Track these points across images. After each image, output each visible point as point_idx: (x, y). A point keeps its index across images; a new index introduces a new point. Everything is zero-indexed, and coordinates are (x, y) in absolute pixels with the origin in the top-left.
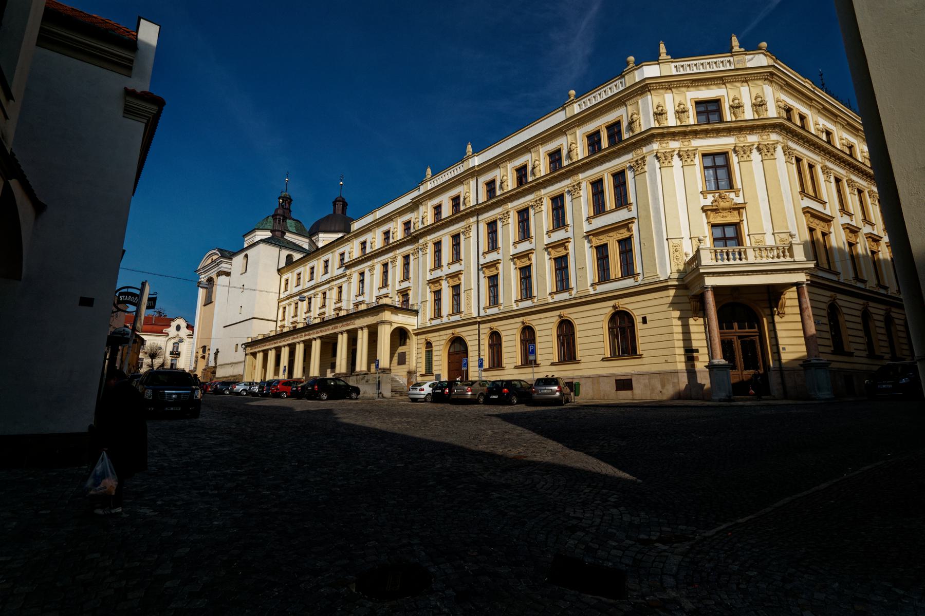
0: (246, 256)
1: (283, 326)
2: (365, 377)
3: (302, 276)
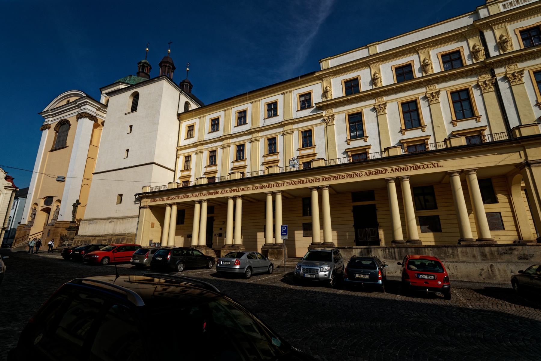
0: (136, 96)
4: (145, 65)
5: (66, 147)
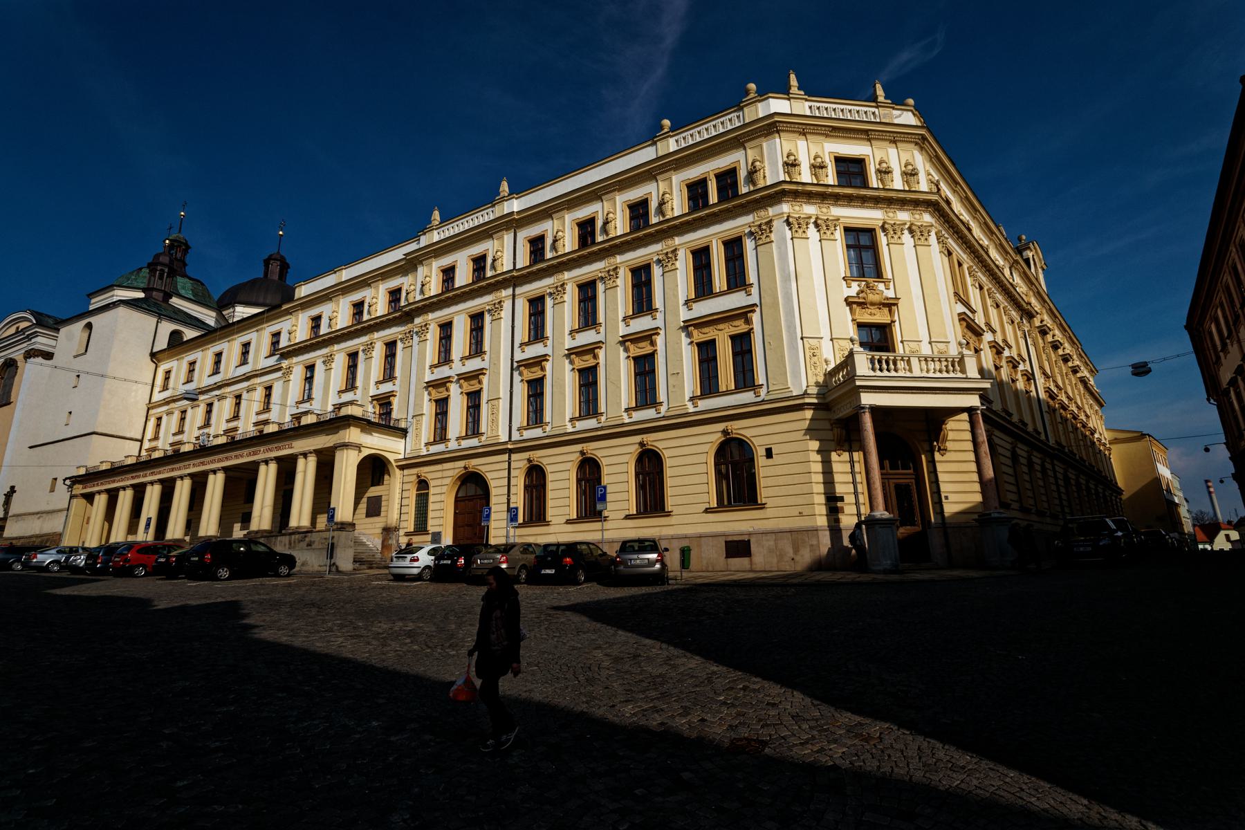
0: (89, 326)
1: (154, 449)
2: (306, 537)
3: (197, 367)
4: (176, 244)
5: (10, 403)
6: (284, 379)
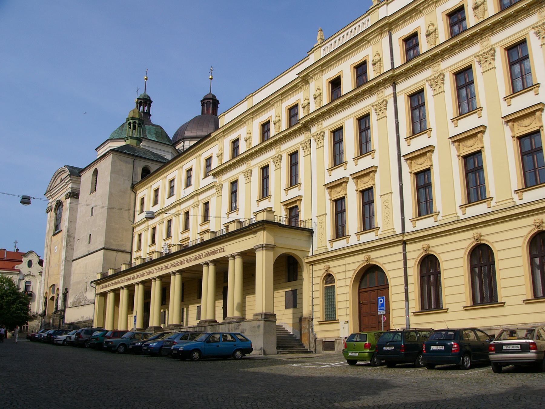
6: (217, 195)
